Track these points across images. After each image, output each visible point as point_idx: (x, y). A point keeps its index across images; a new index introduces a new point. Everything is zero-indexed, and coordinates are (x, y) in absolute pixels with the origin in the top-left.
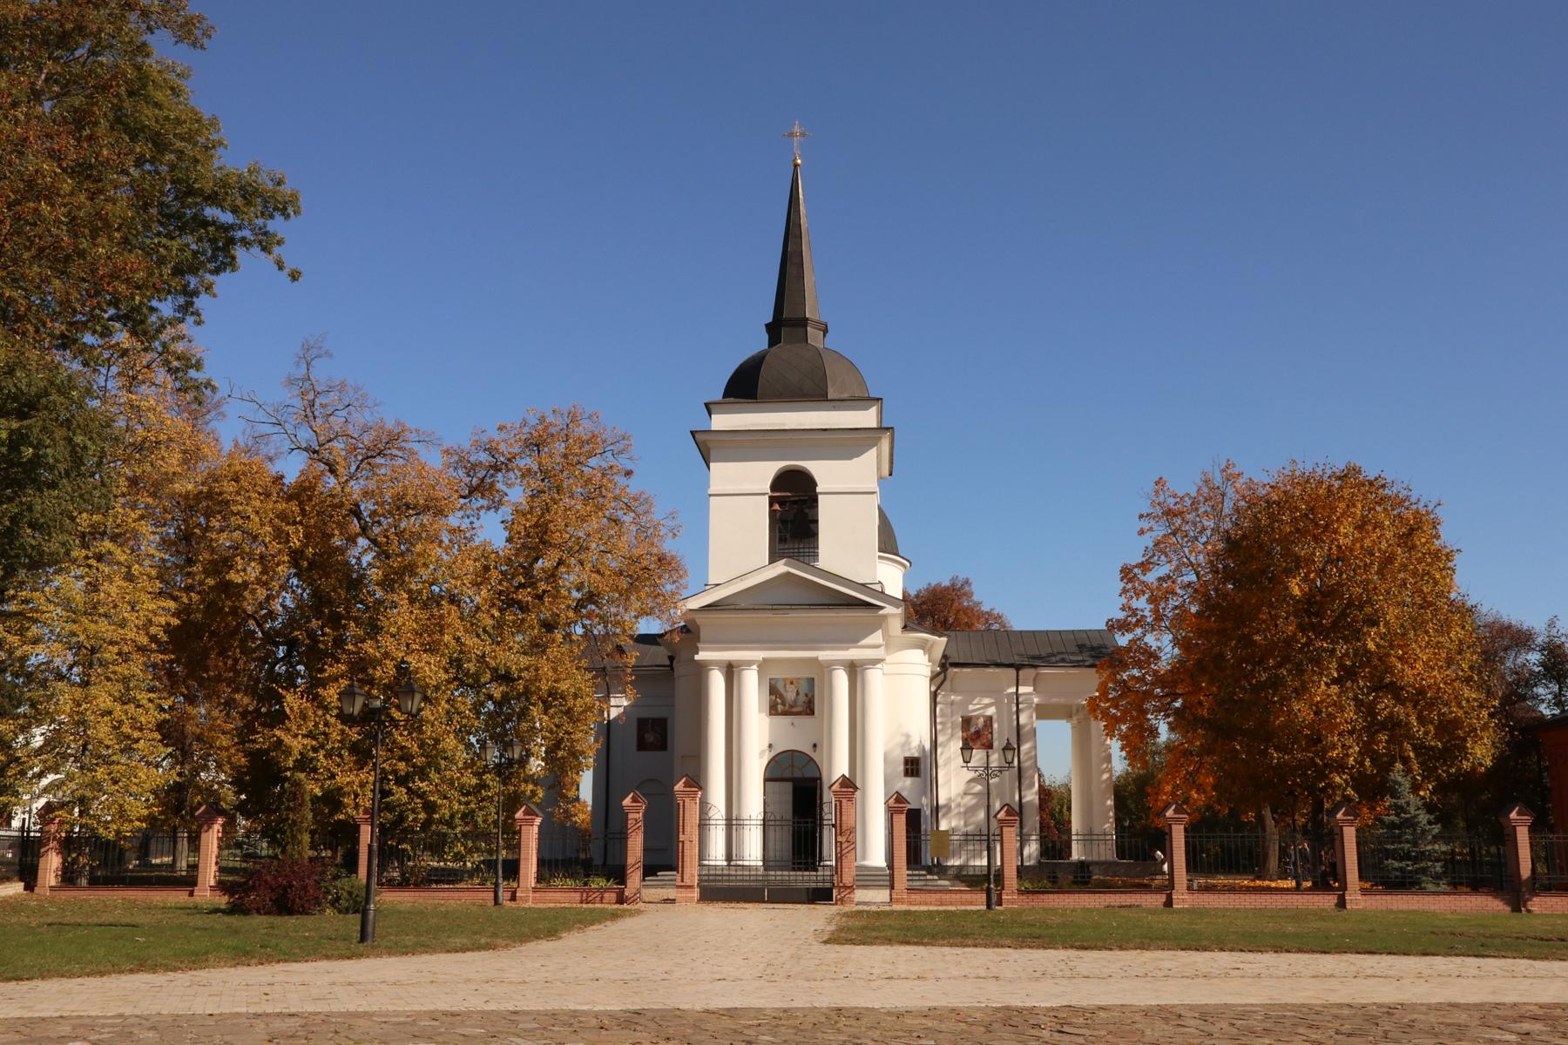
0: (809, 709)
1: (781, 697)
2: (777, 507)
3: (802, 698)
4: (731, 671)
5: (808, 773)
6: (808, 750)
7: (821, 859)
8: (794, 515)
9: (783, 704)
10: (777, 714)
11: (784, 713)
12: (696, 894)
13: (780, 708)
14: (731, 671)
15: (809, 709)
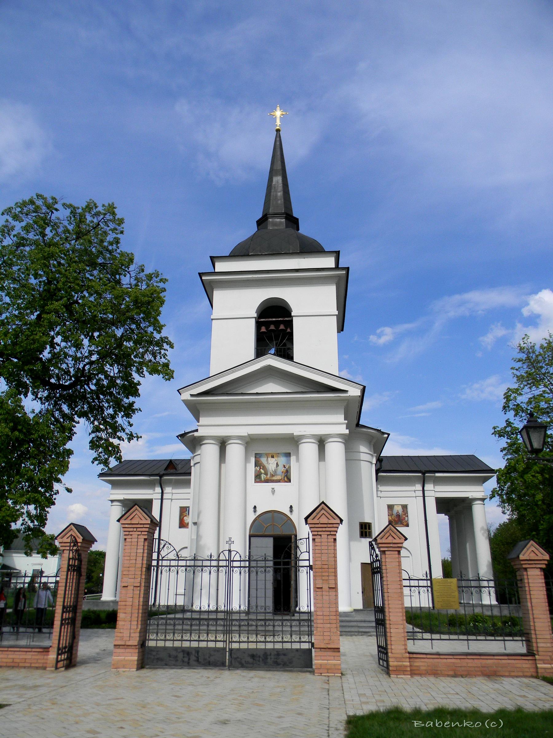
0: (287, 478)
1: (264, 468)
2: (263, 329)
3: (281, 469)
4: (222, 444)
5: (286, 532)
6: (287, 511)
7: (296, 606)
8: (274, 328)
9: (266, 474)
10: (261, 481)
11: (267, 481)
12: (133, 657)
13: (263, 477)
14: (222, 444)
15: (287, 478)
